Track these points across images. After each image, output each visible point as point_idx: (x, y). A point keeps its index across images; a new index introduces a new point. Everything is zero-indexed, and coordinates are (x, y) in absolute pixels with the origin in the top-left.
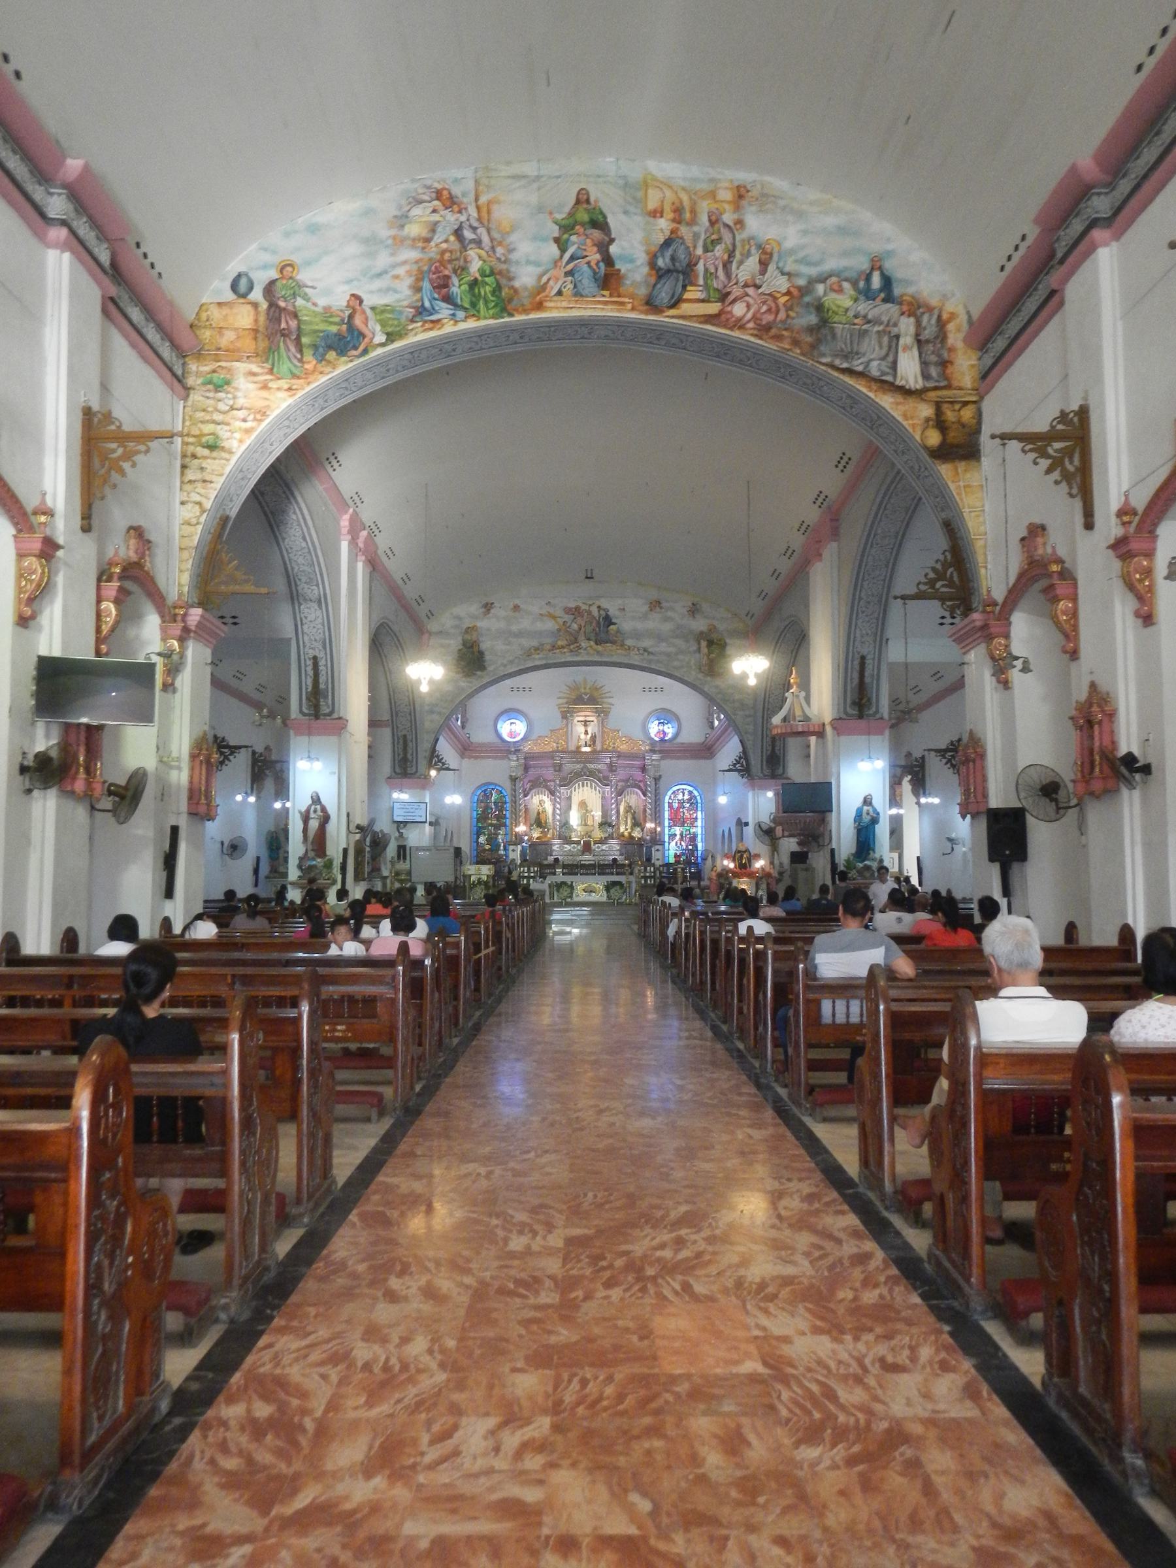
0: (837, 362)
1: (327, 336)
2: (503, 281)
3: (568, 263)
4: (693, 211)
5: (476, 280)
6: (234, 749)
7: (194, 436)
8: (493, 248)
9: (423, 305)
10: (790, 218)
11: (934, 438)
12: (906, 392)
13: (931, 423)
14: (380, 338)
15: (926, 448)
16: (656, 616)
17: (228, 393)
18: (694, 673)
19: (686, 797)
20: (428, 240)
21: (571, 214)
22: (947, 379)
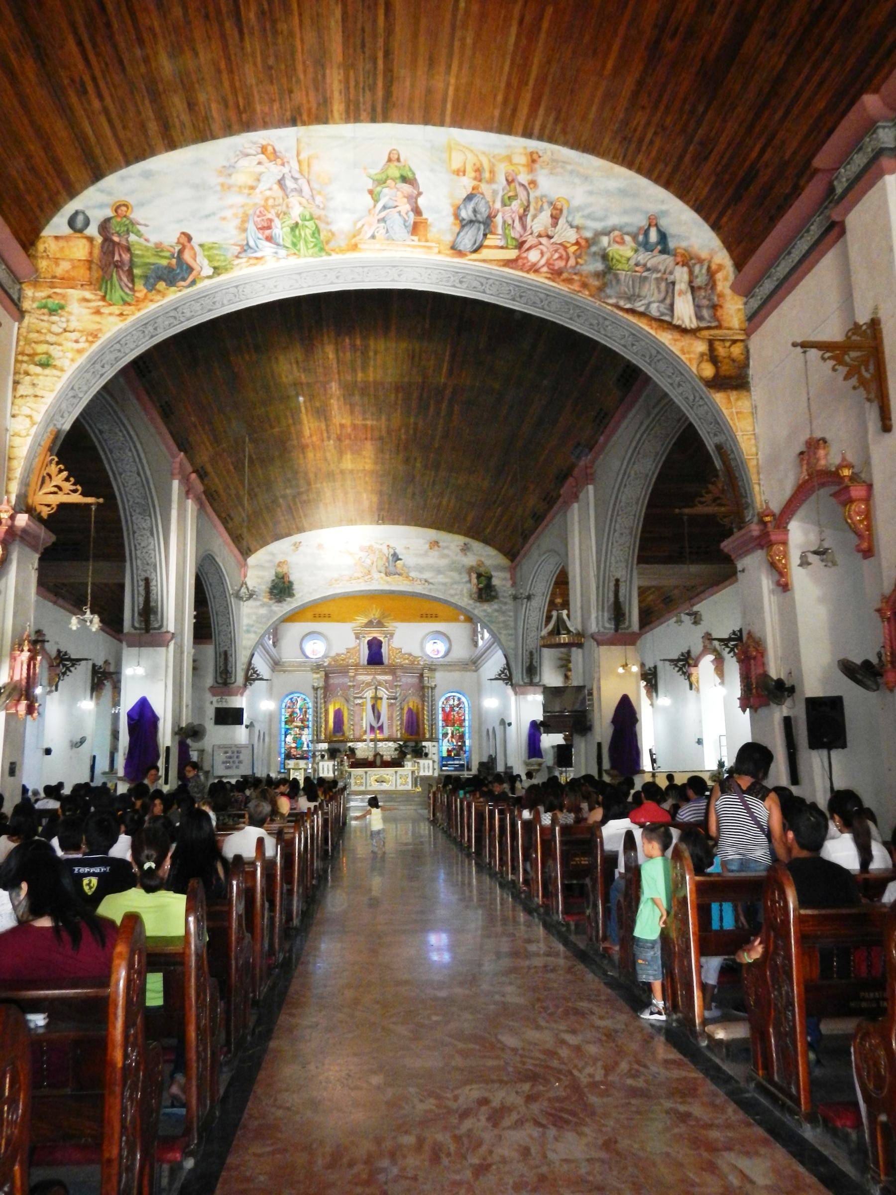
0: (622, 303)
1: (158, 268)
2: (322, 226)
3: (380, 211)
4: (492, 172)
5: (297, 224)
6: (75, 662)
7: (28, 355)
8: (313, 197)
9: (248, 244)
10: (577, 180)
11: (708, 371)
12: (683, 331)
13: (705, 357)
14: (208, 271)
15: (701, 378)
16: (435, 553)
17: (61, 316)
18: (466, 599)
19: (456, 702)
20: (252, 188)
21: (384, 170)
22: (718, 320)
